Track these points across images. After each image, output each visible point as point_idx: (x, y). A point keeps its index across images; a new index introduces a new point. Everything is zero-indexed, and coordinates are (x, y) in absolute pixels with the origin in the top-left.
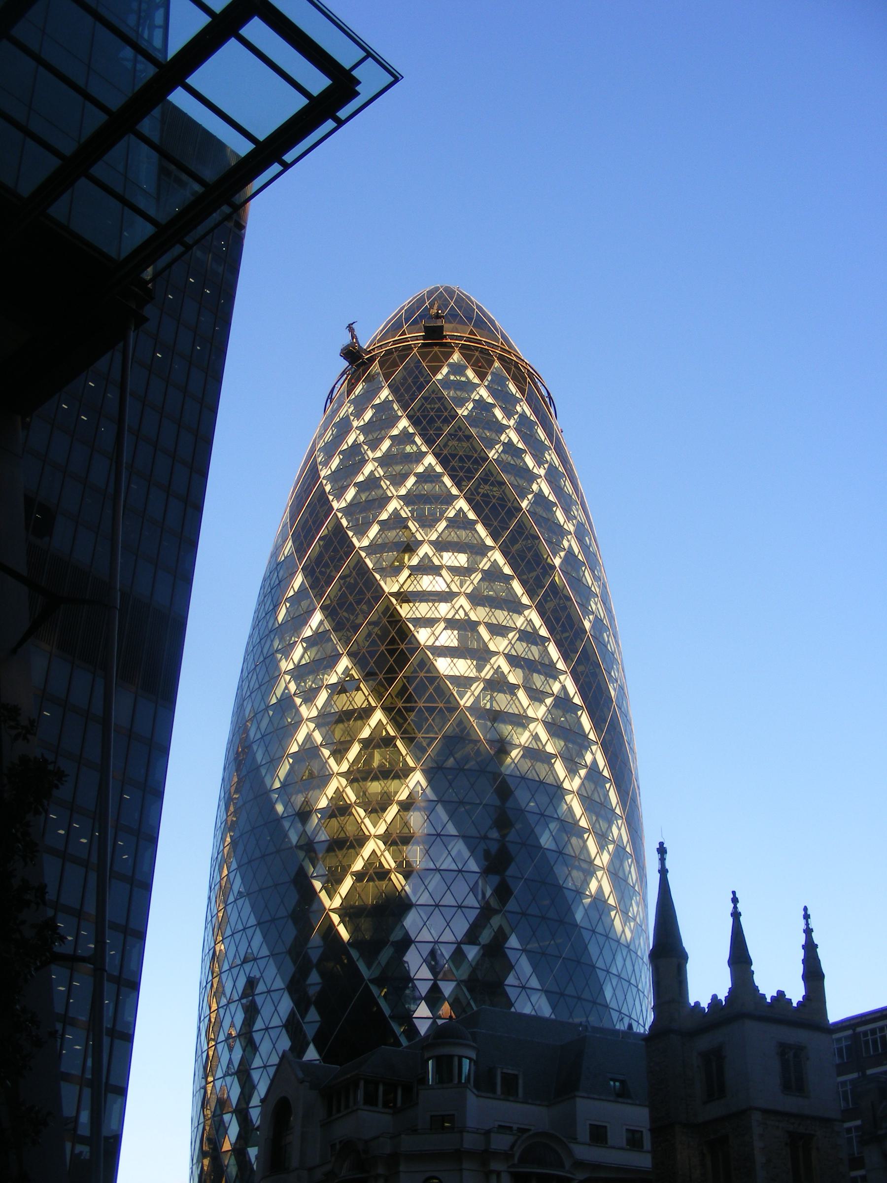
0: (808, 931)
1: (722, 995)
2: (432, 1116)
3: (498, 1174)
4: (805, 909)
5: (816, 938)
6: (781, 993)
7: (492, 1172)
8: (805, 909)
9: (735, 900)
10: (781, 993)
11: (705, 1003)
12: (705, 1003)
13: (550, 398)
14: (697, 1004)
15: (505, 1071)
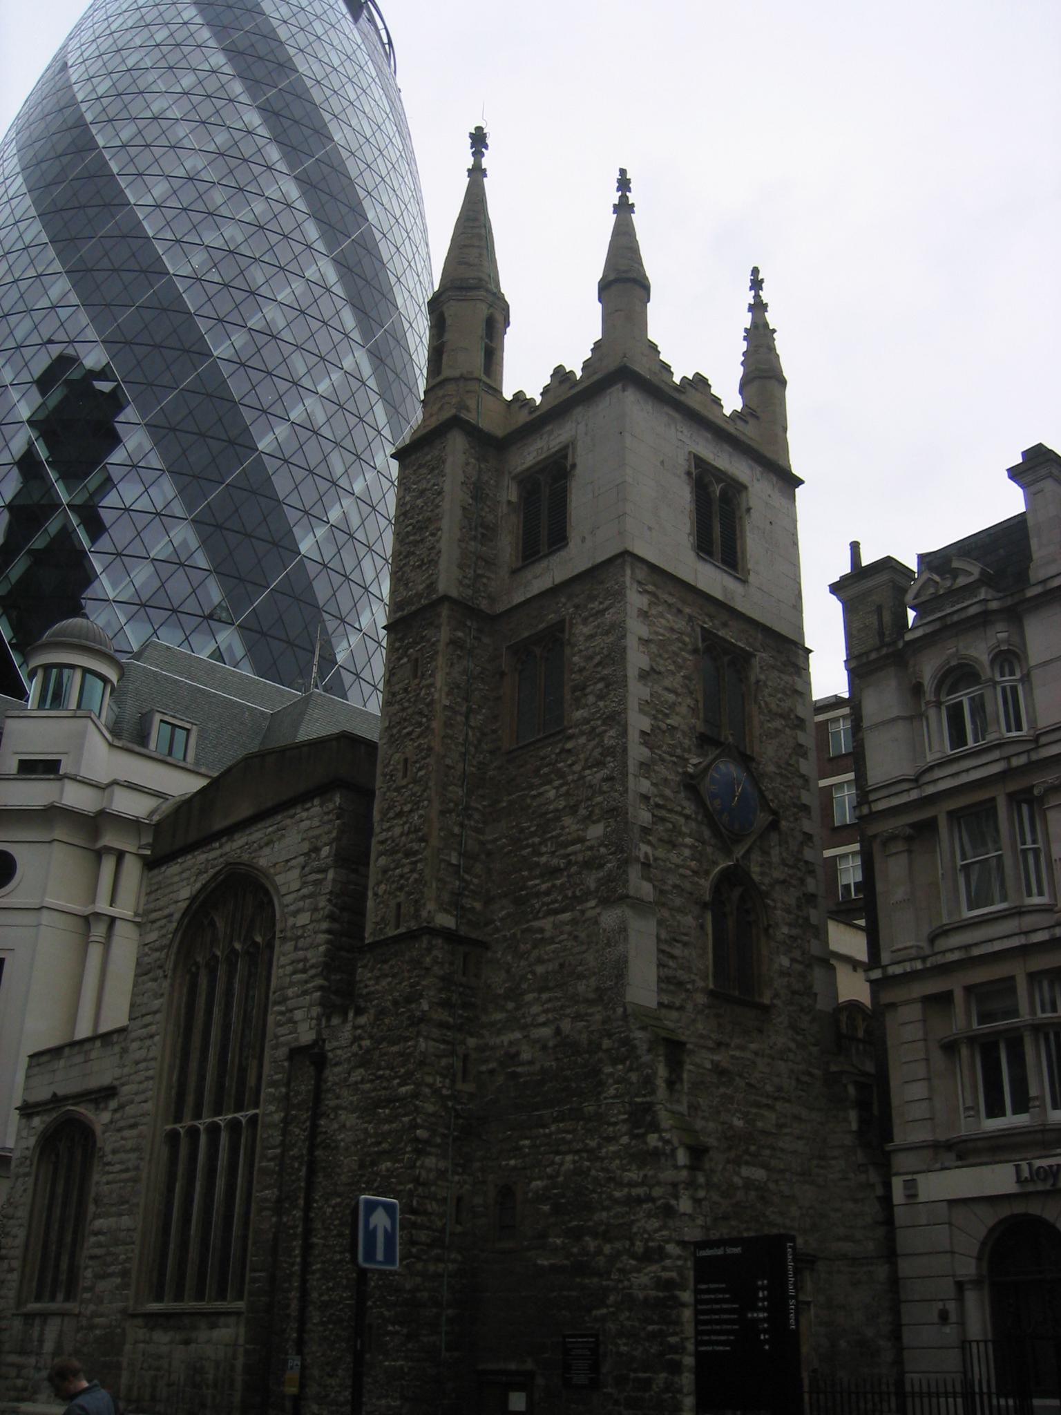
0: (758, 307)
1: (575, 366)
2: (21, 762)
3: (120, 855)
4: (755, 271)
5: (771, 318)
6: (700, 383)
7: (109, 850)
8: (755, 271)
9: (624, 184)
10: (700, 383)
11: (534, 393)
12: (534, 393)
13: (390, 43)
14: (519, 396)
15: (167, 718)
